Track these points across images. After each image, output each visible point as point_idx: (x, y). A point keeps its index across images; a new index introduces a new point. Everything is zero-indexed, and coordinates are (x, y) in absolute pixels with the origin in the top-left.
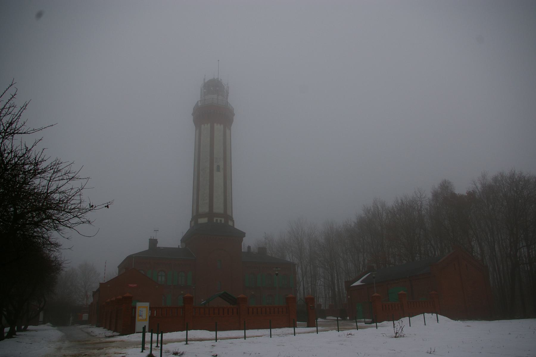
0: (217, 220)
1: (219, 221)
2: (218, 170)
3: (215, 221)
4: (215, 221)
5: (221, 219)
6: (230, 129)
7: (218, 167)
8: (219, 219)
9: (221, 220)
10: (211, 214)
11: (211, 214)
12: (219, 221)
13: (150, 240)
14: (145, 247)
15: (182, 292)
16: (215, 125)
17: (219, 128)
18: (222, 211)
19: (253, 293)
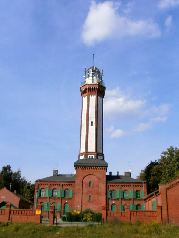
0: (90, 156)
1: (91, 157)
2: (92, 125)
3: (88, 157)
4: (88, 157)
5: (92, 155)
7: (92, 122)
8: (91, 156)
9: (92, 157)
10: (87, 153)
12: (91, 157)
13: (54, 170)
14: (51, 174)
15: (67, 202)
16: (90, 96)
19: (114, 203)
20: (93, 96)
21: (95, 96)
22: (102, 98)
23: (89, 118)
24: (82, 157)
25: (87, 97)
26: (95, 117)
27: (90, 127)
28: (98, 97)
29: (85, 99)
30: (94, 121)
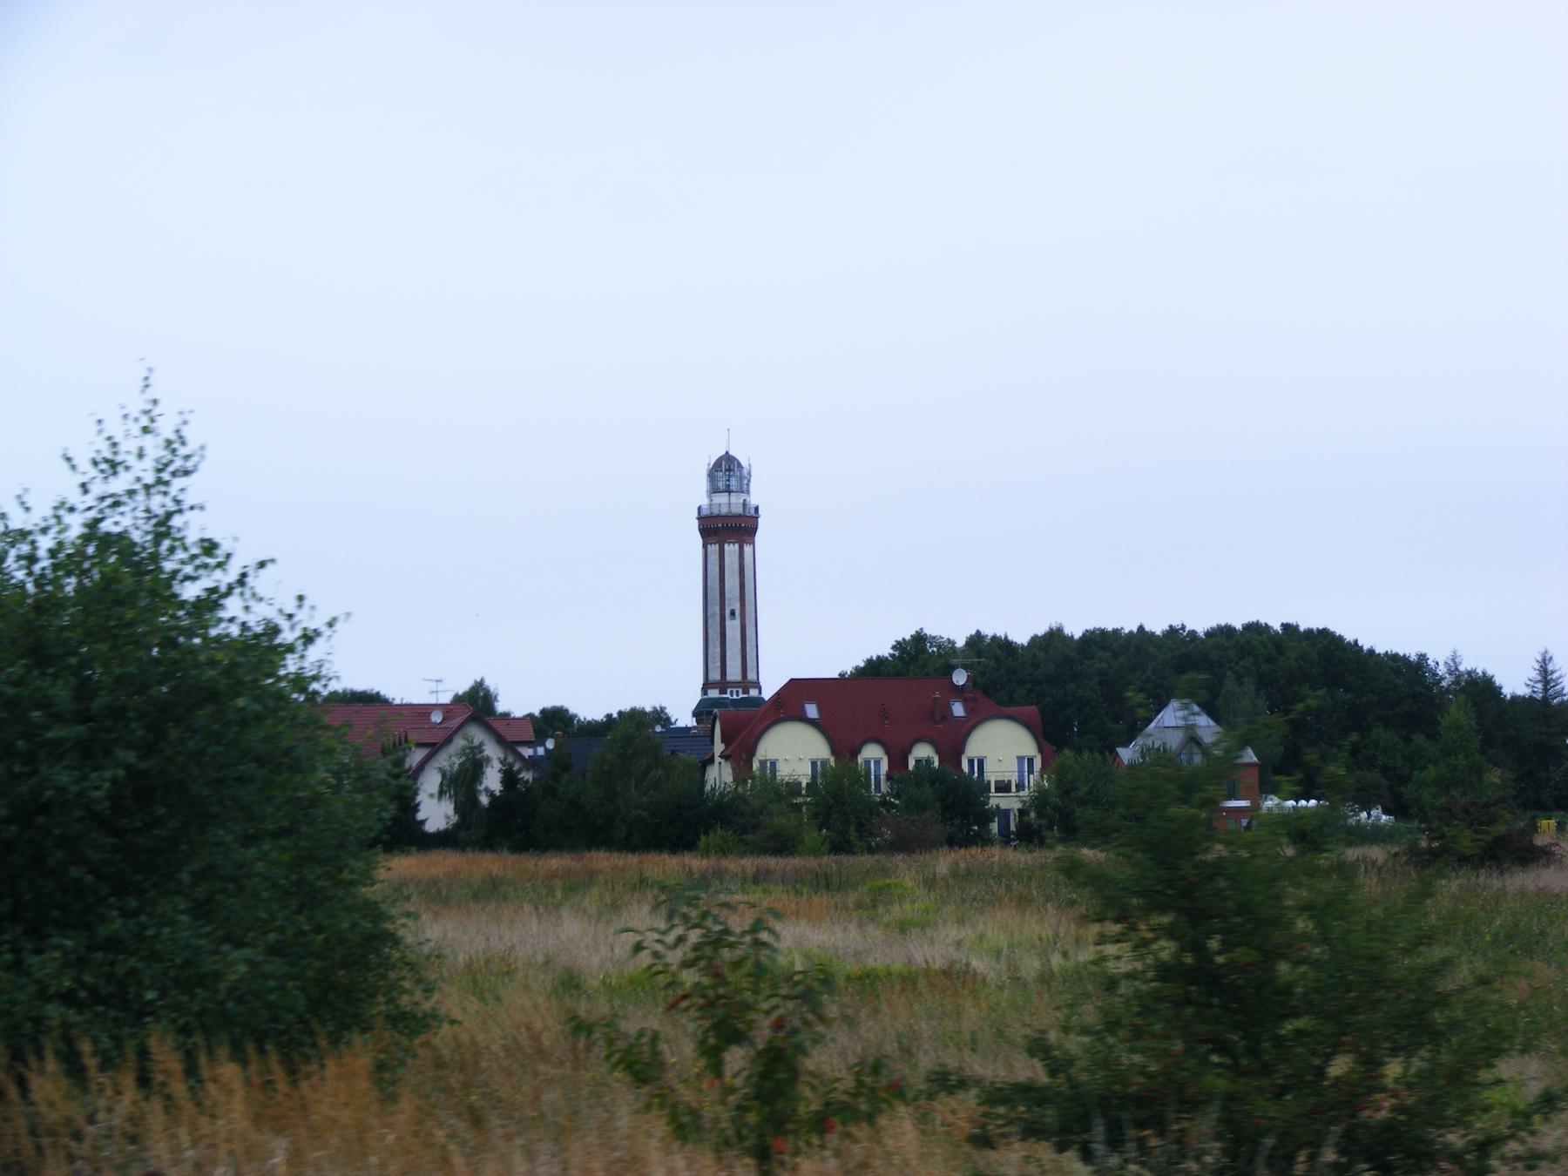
0: (732, 692)
6: (753, 543)
7: (733, 613)
8: (735, 690)
9: (737, 692)
10: (723, 685)
11: (723, 685)
16: (726, 546)
17: (731, 549)
18: (739, 678)
20: (731, 545)
21: (737, 546)
22: (752, 546)
23: (724, 600)
24: (714, 693)
25: (717, 546)
26: (738, 599)
27: (729, 623)
28: (745, 545)
29: (714, 549)
30: (737, 607)
